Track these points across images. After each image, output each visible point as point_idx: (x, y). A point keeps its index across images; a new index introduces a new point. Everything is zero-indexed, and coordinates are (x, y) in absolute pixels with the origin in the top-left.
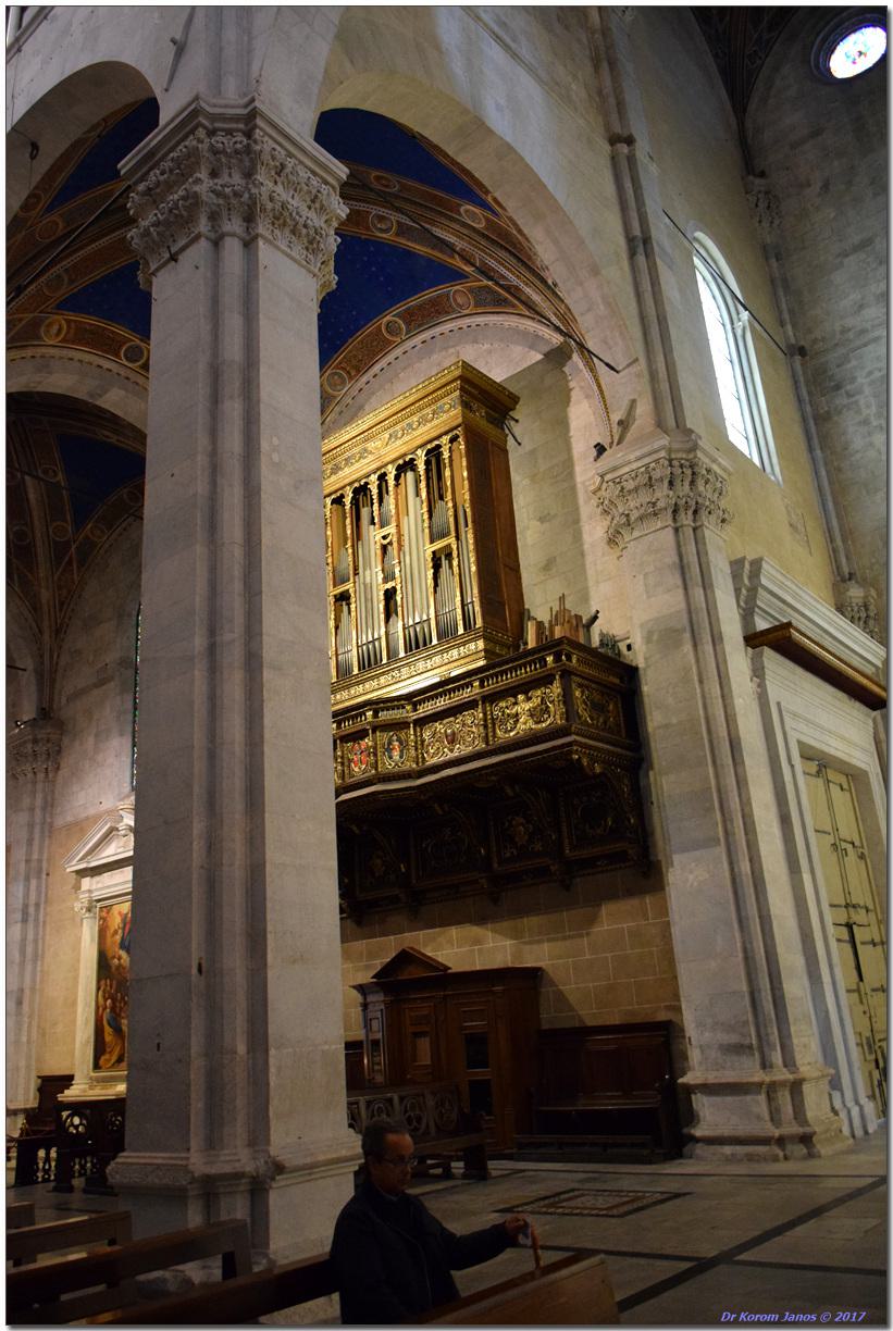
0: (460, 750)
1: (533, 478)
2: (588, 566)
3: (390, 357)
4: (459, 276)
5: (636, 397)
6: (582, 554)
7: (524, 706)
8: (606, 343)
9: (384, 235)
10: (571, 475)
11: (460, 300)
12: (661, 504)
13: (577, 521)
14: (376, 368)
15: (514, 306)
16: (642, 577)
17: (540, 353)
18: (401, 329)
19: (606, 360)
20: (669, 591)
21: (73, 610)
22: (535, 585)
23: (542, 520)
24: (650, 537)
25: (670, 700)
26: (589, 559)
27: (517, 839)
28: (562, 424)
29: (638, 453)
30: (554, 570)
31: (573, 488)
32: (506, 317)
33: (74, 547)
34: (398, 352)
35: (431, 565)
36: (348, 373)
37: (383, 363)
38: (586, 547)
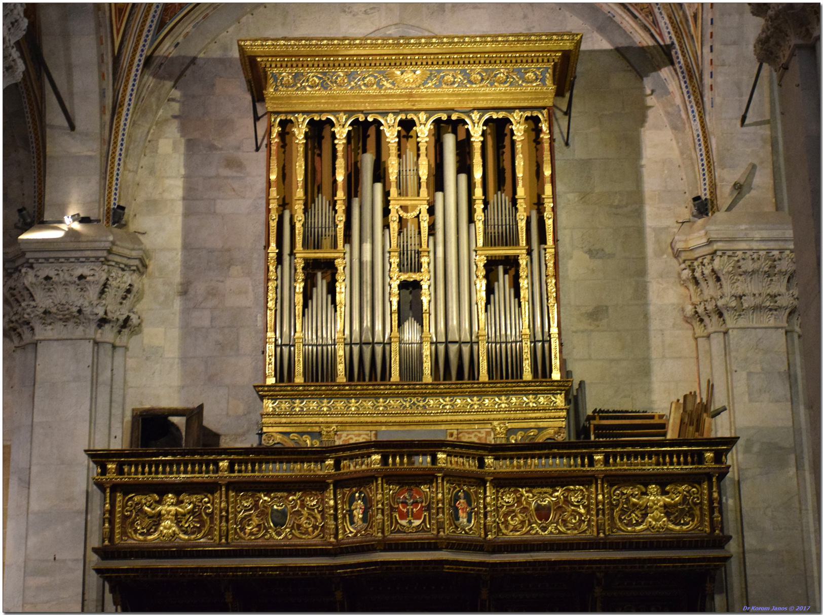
0: (551, 531)
1: (584, 197)
2: (652, 334)
5: (756, 162)
6: (646, 317)
7: (654, 498)
8: (739, 88)
10: (638, 213)
13: (642, 273)
16: (744, 374)
17: (610, 41)
19: (748, 115)
20: (777, 401)
22: (576, 332)
23: (592, 253)
24: (760, 333)
26: (655, 325)
29: (765, 234)
30: (605, 321)
31: (640, 232)
35: (484, 273)
38: (652, 309)
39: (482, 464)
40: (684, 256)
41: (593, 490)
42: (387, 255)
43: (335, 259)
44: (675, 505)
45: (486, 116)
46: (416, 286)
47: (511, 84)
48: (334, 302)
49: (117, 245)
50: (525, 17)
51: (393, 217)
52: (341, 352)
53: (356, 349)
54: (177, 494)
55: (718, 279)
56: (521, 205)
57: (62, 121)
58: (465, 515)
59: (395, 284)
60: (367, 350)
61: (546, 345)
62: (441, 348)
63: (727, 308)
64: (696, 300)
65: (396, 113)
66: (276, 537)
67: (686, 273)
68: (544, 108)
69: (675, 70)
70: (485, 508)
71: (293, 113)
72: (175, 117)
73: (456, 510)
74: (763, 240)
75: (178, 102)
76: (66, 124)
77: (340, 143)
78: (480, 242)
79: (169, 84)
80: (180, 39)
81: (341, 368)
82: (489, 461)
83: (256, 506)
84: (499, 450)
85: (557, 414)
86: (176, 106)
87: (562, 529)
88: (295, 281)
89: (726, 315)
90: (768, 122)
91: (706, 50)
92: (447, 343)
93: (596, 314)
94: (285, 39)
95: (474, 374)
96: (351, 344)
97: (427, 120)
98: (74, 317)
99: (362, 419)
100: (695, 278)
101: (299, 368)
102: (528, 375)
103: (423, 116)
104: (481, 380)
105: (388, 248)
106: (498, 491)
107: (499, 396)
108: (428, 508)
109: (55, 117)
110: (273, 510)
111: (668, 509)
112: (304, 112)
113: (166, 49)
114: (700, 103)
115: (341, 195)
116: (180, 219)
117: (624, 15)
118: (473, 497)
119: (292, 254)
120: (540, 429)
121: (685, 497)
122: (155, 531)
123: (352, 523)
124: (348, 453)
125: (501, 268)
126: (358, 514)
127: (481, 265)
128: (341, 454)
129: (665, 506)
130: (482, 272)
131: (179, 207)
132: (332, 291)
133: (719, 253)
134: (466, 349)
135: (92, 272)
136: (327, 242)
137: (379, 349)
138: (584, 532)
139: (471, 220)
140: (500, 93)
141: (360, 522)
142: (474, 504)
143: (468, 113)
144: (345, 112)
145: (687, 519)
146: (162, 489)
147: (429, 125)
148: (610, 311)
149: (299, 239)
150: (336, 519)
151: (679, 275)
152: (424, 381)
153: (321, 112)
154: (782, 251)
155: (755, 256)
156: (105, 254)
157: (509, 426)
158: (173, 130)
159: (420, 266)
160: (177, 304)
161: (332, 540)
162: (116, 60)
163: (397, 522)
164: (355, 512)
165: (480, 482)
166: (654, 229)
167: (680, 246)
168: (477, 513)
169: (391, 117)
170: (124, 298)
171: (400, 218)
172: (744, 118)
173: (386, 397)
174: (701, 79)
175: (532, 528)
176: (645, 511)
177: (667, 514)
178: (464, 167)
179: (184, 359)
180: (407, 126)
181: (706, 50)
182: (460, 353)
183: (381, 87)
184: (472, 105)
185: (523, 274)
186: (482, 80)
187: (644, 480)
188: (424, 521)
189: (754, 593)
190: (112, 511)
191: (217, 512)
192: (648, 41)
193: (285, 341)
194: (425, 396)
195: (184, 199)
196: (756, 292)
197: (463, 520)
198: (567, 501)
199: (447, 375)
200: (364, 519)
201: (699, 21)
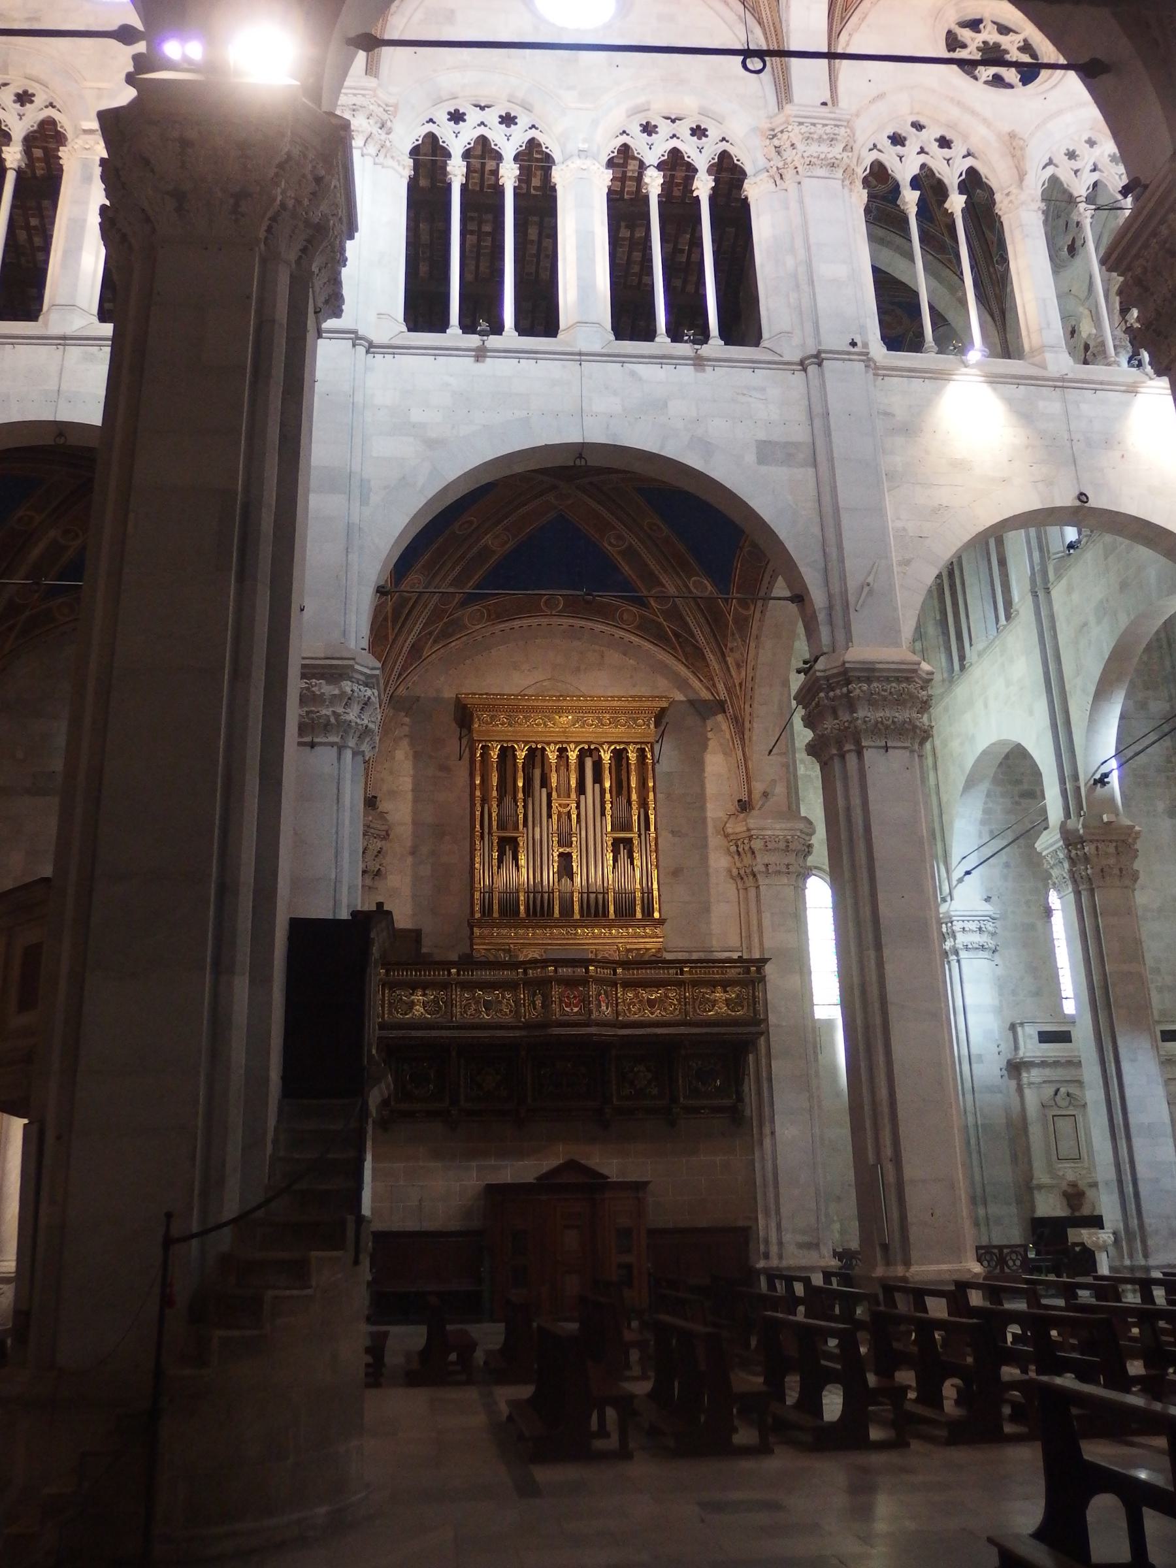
0: (656, 1015)
3: (534, 621)
4: (641, 602)
6: (707, 874)
7: (719, 994)
9: (609, 548)
10: (703, 808)
11: (625, 616)
12: (792, 869)
13: (705, 846)
14: (516, 624)
15: (674, 648)
17: (686, 696)
18: (557, 605)
26: (713, 880)
28: (698, 765)
29: (784, 826)
32: (663, 652)
34: (544, 621)
36: (489, 615)
37: (525, 622)
38: (711, 870)
39: (615, 973)
40: (731, 838)
41: (682, 989)
42: (550, 835)
43: (517, 838)
44: (731, 999)
45: (613, 747)
46: (569, 855)
47: (628, 727)
48: (517, 865)
50: (631, 677)
51: (554, 810)
52: (522, 898)
53: (531, 895)
54: (424, 989)
55: (753, 853)
56: (635, 806)
58: (604, 1005)
59: (556, 854)
60: (539, 896)
61: (650, 895)
62: (585, 895)
63: (760, 872)
64: (739, 865)
65: (556, 743)
66: (486, 1017)
67: (733, 849)
68: (648, 743)
69: (726, 716)
70: (617, 1000)
71: (490, 741)
72: (405, 736)
73: (600, 1001)
75: (407, 725)
77: (520, 762)
78: (609, 829)
79: (403, 714)
81: (522, 908)
82: (619, 971)
83: (474, 997)
84: (626, 964)
85: (658, 940)
86: (406, 729)
87: (664, 1014)
88: (492, 851)
89: (758, 876)
90: (784, 753)
91: (747, 706)
92: (588, 893)
93: (676, 873)
94: (486, 694)
95: (605, 913)
96: (528, 892)
97: (575, 748)
99: (536, 942)
100: (738, 851)
101: (496, 907)
102: (639, 915)
103: (572, 746)
104: (610, 918)
105: (551, 831)
106: (624, 990)
107: (621, 928)
108: (583, 1001)
110: (484, 1000)
111: (728, 1002)
112: (497, 741)
113: (402, 691)
114: (742, 739)
115: (520, 795)
116: (410, 804)
117: (694, 679)
118: (609, 993)
119: (490, 833)
120: (647, 949)
121: (738, 995)
122: (411, 1011)
123: (535, 1008)
124: (533, 965)
125: (622, 845)
126: (539, 1003)
127: (609, 843)
128: (528, 966)
129: (726, 1000)
130: (610, 849)
131: (410, 796)
132: (516, 858)
133: (754, 837)
134: (600, 896)
136: (510, 826)
137: (546, 896)
138: (678, 1015)
139: (603, 814)
140: (622, 733)
141: (540, 1009)
142: (610, 998)
143: (601, 744)
144: (523, 742)
145: (740, 1008)
146: (413, 987)
147: (576, 752)
148: (685, 870)
149: (495, 824)
150: (524, 1007)
151: (728, 849)
152: (575, 918)
153: (508, 741)
154: (793, 836)
155: (777, 840)
157: (628, 947)
158: (405, 743)
159: (572, 843)
160: (410, 860)
161: (523, 1020)
163: (564, 1009)
164: (537, 1002)
165: (614, 984)
166: (713, 819)
167: (730, 831)
168: (612, 1004)
169: (552, 746)
170: (376, 856)
171: (559, 811)
172: (771, 751)
173: (551, 927)
174: (743, 724)
175: (645, 1013)
176: (714, 1003)
177: (727, 1005)
178: (598, 779)
179: (414, 896)
180: (562, 751)
181: (747, 706)
182: (597, 898)
183: (546, 725)
184: (604, 740)
185: (636, 849)
186: (610, 723)
187: (713, 984)
188: (581, 1009)
191: (449, 1000)
192: (708, 696)
193: (487, 890)
194: (576, 927)
195: (413, 790)
196: (778, 863)
197: (604, 1008)
198: (667, 997)
199: (589, 915)
200: (543, 1007)
201: (743, 687)
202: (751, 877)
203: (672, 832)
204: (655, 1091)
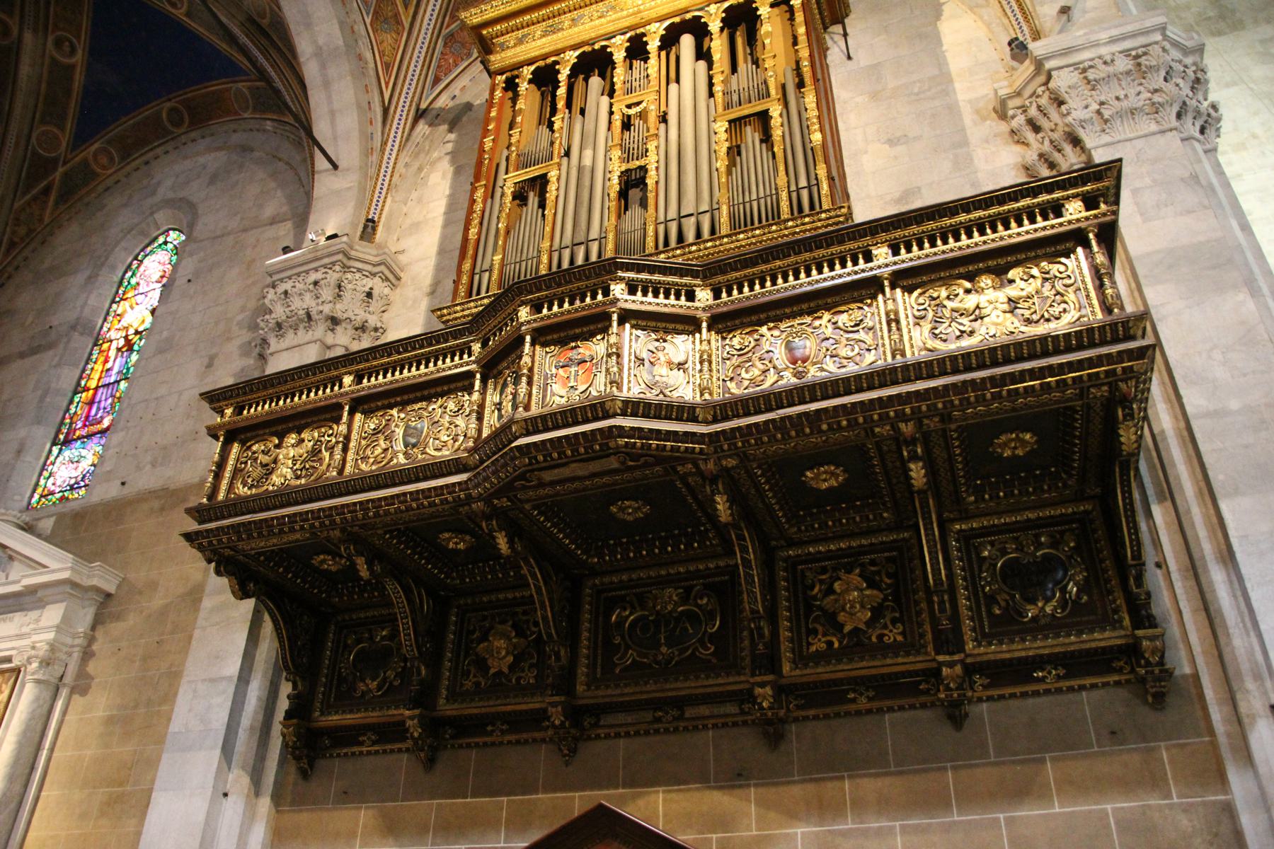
13: (964, 143)
20: (1189, 212)
21: (26, 259)
25: (1220, 373)
27: (842, 617)
33: (61, 170)
49: (356, 250)
57: (328, 165)
61: (815, 189)
63: (1082, 123)
74: (1113, 41)
76: (329, 166)
80: (457, 93)
89: (1082, 134)
98: (302, 321)
109: (321, 163)
113: (443, 102)
131: (439, 222)
135: (324, 276)
148: (923, 191)
153: (545, 57)
156: (340, 257)
162: (386, 111)
166: (970, 102)
176: (977, 315)
189: (1221, 477)
190: (221, 465)
202: (1068, 148)
203: (891, 142)
204: (894, 635)
